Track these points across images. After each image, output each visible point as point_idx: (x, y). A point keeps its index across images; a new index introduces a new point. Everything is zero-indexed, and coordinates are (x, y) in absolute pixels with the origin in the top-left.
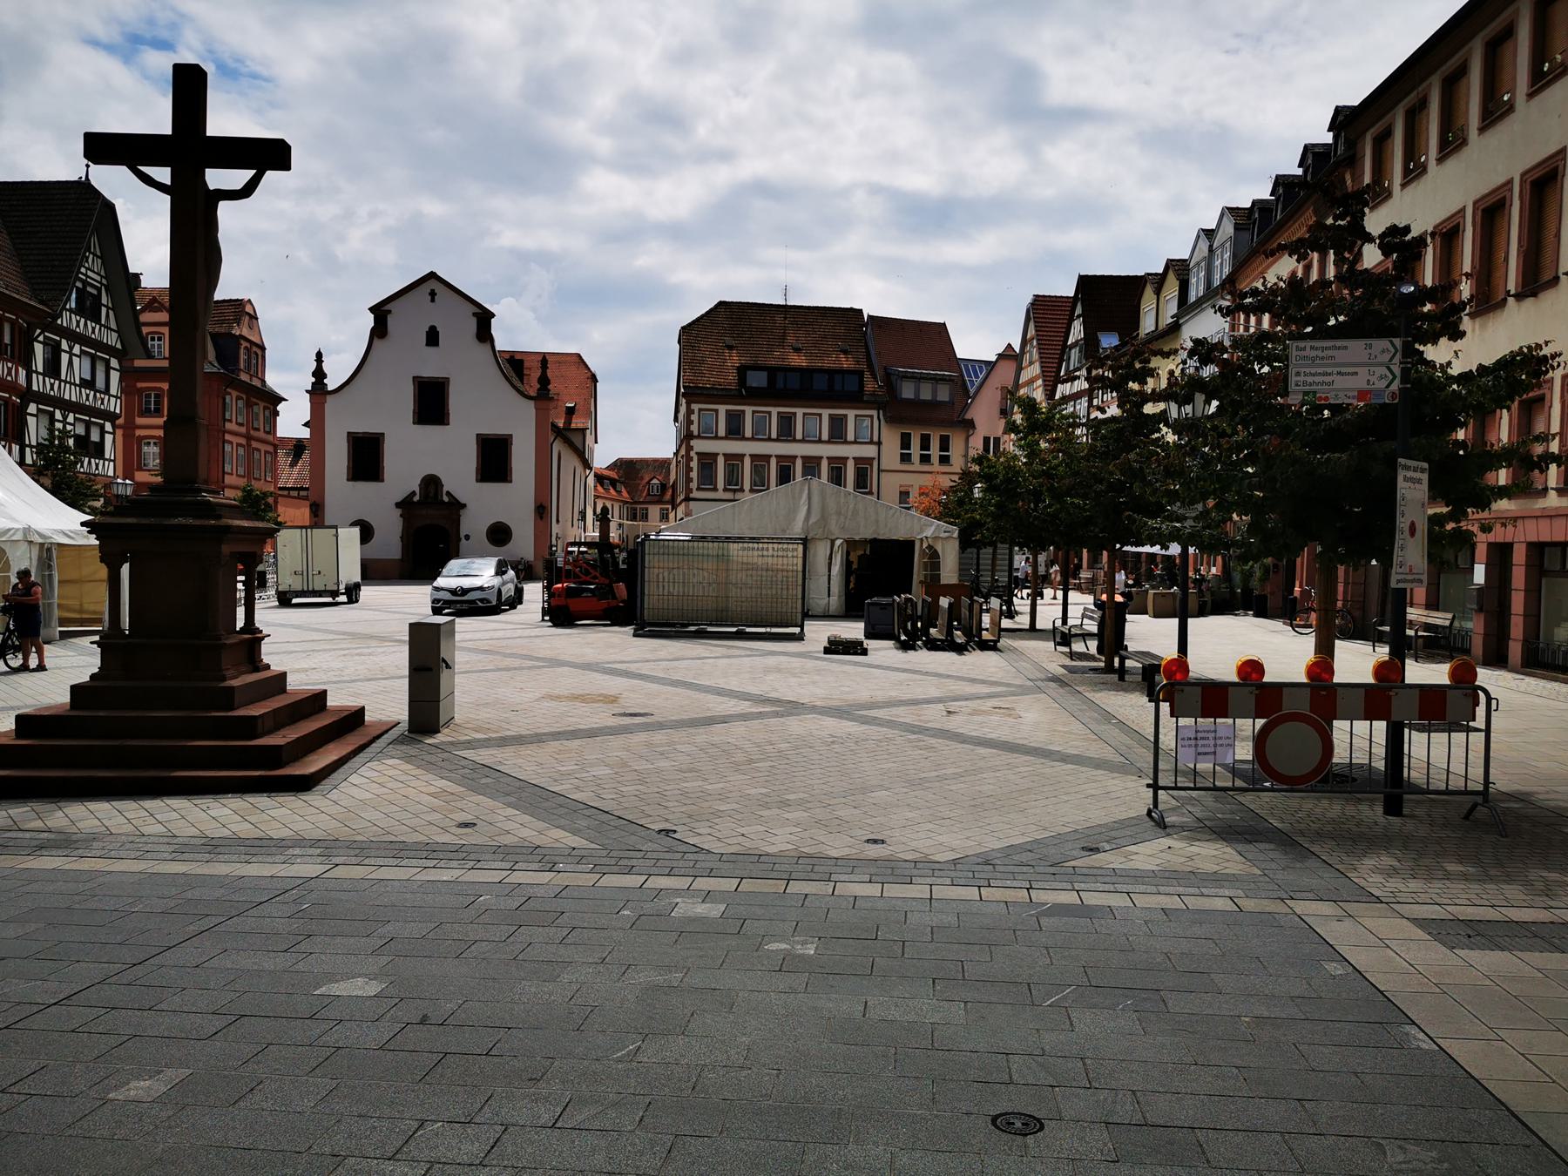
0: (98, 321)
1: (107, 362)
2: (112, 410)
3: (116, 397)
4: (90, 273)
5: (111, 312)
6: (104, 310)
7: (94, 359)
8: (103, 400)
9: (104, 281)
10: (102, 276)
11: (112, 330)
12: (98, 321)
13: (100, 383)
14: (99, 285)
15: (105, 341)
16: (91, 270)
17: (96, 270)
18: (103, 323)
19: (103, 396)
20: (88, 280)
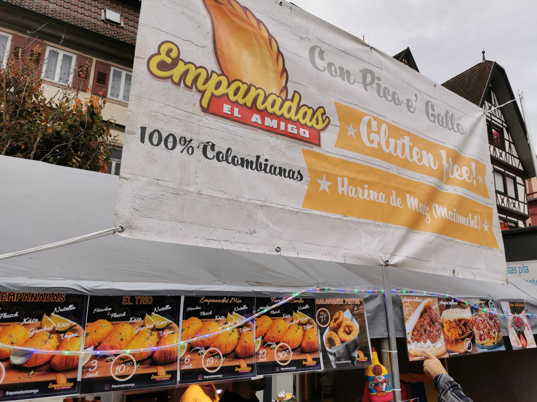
0: (504, 149)
1: (514, 180)
2: (522, 211)
3: (524, 203)
4: (493, 117)
5: (512, 146)
6: (507, 143)
7: (504, 176)
8: (514, 204)
9: (504, 124)
10: (503, 121)
11: (514, 157)
12: (504, 149)
13: (511, 192)
14: (501, 127)
15: (510, 163)
16: (494, 115)
17: (498, 116)
18: (507, 150)
19: (514, 201)
20: (493, 121)
